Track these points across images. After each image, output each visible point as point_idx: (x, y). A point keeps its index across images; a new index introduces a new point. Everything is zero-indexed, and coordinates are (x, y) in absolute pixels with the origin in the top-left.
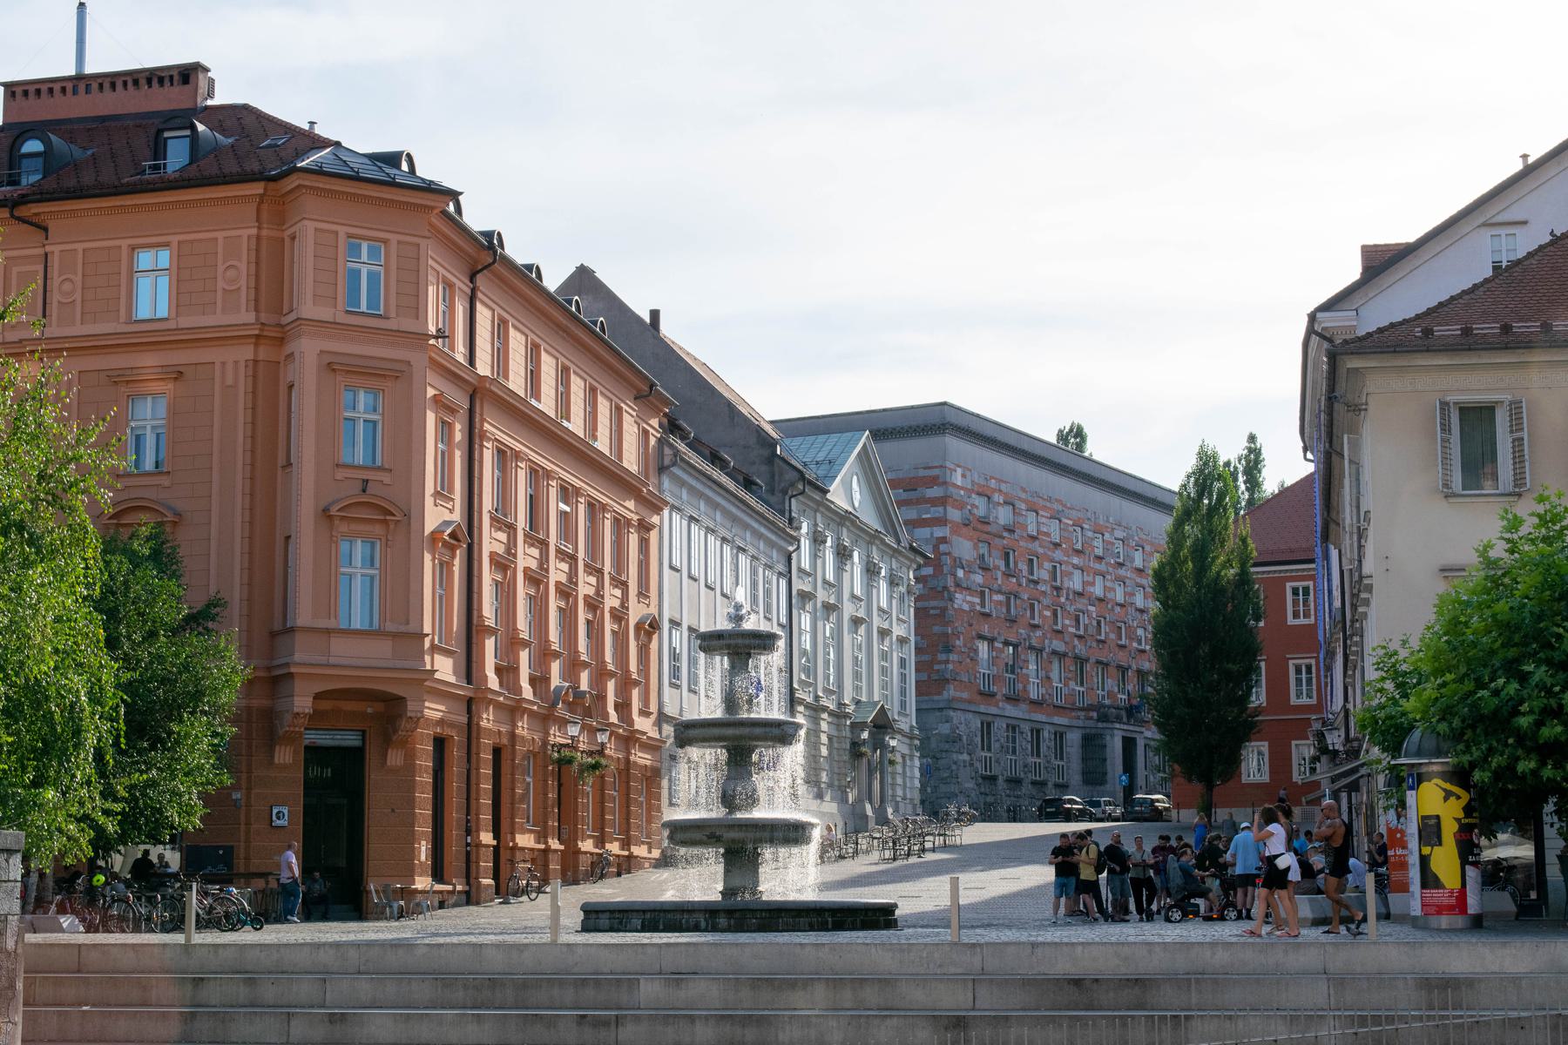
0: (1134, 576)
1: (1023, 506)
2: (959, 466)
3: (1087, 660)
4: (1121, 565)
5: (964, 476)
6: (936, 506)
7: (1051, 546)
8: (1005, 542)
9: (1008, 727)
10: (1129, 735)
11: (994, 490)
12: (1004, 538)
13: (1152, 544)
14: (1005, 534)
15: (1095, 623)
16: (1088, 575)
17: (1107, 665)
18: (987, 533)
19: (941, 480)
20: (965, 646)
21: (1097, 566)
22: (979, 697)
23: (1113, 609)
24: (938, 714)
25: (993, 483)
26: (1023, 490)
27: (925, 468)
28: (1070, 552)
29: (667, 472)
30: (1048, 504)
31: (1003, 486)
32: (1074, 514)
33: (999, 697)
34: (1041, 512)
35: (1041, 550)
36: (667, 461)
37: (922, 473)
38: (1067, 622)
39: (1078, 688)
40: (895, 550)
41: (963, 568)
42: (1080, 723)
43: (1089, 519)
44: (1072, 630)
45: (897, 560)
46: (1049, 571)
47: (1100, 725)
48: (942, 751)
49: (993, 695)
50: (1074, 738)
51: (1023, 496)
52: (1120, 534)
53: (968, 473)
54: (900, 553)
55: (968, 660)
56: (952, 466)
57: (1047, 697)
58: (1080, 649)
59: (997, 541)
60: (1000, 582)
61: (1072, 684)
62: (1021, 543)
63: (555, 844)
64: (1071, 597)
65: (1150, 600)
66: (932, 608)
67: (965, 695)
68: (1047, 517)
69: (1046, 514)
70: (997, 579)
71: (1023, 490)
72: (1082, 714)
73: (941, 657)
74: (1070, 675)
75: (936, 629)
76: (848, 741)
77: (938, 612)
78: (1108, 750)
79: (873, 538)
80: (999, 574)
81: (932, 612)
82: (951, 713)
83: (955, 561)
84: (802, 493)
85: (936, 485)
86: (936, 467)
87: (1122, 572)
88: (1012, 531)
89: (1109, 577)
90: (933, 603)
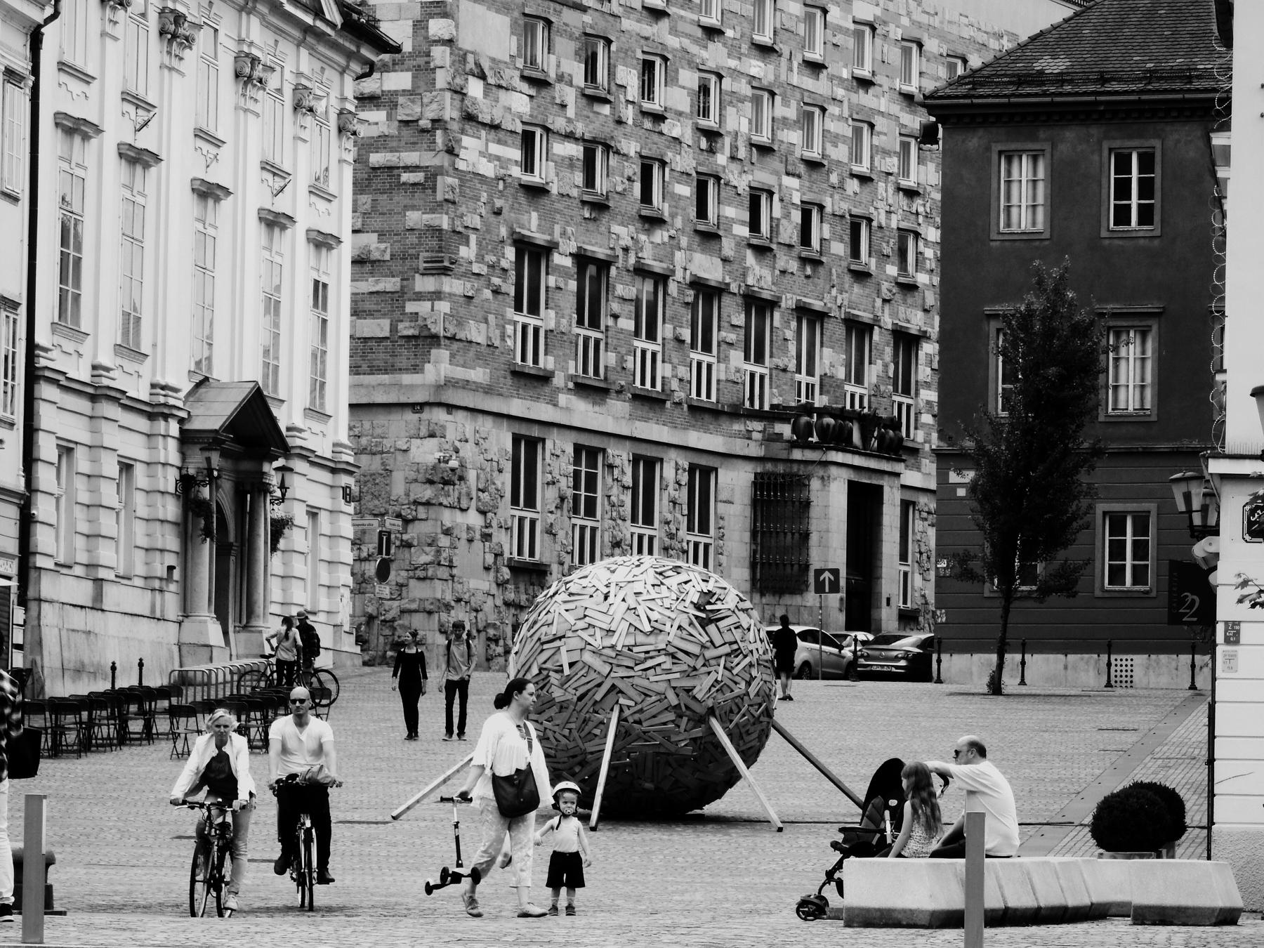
0: (896, 108)
3: (773, 304)
4: (865, 84)
7: (699, 33)
8: (587, 18)
9: (578, 449)
13: (942, 36)
15: (797, 216)
16: (786, 103)
20: (480, 258)
21: (808, 82)
22: (509, 381)
23: (842, 187)
24: (410, 416)
28: (745, 48)
33: (559, 380)
35: (673, 42)
38: (730, 212)
39: (751, 367)
40: (307, 30)
41: (482, 76)
42: (755, 450)
44: (744, 231)
46: (690, 91)
47: (797, 454)
48: (416, 503)
49: (544, 378)
54: (320, 36)
55: (487, 294)
57: (675, 385)
58: (760, 276)
60: (571, 112)
61: (736, 356)
62: (627, 24)
64: (742, 153)
65: (931, 167)
66: (407, 168)
67: (478, 375)
70: (563, 106)
72: (757, 426)
73: (424, 284)
74: (732, 337)
75: (414, 218)
77: (418, 177)
78: (815, 512)
80: (570, 96)
81: (405, 177)
82: (440, 415)
83: (464, 59)
87: (866, 99)
89: (833, 109)
90: (411, 158)
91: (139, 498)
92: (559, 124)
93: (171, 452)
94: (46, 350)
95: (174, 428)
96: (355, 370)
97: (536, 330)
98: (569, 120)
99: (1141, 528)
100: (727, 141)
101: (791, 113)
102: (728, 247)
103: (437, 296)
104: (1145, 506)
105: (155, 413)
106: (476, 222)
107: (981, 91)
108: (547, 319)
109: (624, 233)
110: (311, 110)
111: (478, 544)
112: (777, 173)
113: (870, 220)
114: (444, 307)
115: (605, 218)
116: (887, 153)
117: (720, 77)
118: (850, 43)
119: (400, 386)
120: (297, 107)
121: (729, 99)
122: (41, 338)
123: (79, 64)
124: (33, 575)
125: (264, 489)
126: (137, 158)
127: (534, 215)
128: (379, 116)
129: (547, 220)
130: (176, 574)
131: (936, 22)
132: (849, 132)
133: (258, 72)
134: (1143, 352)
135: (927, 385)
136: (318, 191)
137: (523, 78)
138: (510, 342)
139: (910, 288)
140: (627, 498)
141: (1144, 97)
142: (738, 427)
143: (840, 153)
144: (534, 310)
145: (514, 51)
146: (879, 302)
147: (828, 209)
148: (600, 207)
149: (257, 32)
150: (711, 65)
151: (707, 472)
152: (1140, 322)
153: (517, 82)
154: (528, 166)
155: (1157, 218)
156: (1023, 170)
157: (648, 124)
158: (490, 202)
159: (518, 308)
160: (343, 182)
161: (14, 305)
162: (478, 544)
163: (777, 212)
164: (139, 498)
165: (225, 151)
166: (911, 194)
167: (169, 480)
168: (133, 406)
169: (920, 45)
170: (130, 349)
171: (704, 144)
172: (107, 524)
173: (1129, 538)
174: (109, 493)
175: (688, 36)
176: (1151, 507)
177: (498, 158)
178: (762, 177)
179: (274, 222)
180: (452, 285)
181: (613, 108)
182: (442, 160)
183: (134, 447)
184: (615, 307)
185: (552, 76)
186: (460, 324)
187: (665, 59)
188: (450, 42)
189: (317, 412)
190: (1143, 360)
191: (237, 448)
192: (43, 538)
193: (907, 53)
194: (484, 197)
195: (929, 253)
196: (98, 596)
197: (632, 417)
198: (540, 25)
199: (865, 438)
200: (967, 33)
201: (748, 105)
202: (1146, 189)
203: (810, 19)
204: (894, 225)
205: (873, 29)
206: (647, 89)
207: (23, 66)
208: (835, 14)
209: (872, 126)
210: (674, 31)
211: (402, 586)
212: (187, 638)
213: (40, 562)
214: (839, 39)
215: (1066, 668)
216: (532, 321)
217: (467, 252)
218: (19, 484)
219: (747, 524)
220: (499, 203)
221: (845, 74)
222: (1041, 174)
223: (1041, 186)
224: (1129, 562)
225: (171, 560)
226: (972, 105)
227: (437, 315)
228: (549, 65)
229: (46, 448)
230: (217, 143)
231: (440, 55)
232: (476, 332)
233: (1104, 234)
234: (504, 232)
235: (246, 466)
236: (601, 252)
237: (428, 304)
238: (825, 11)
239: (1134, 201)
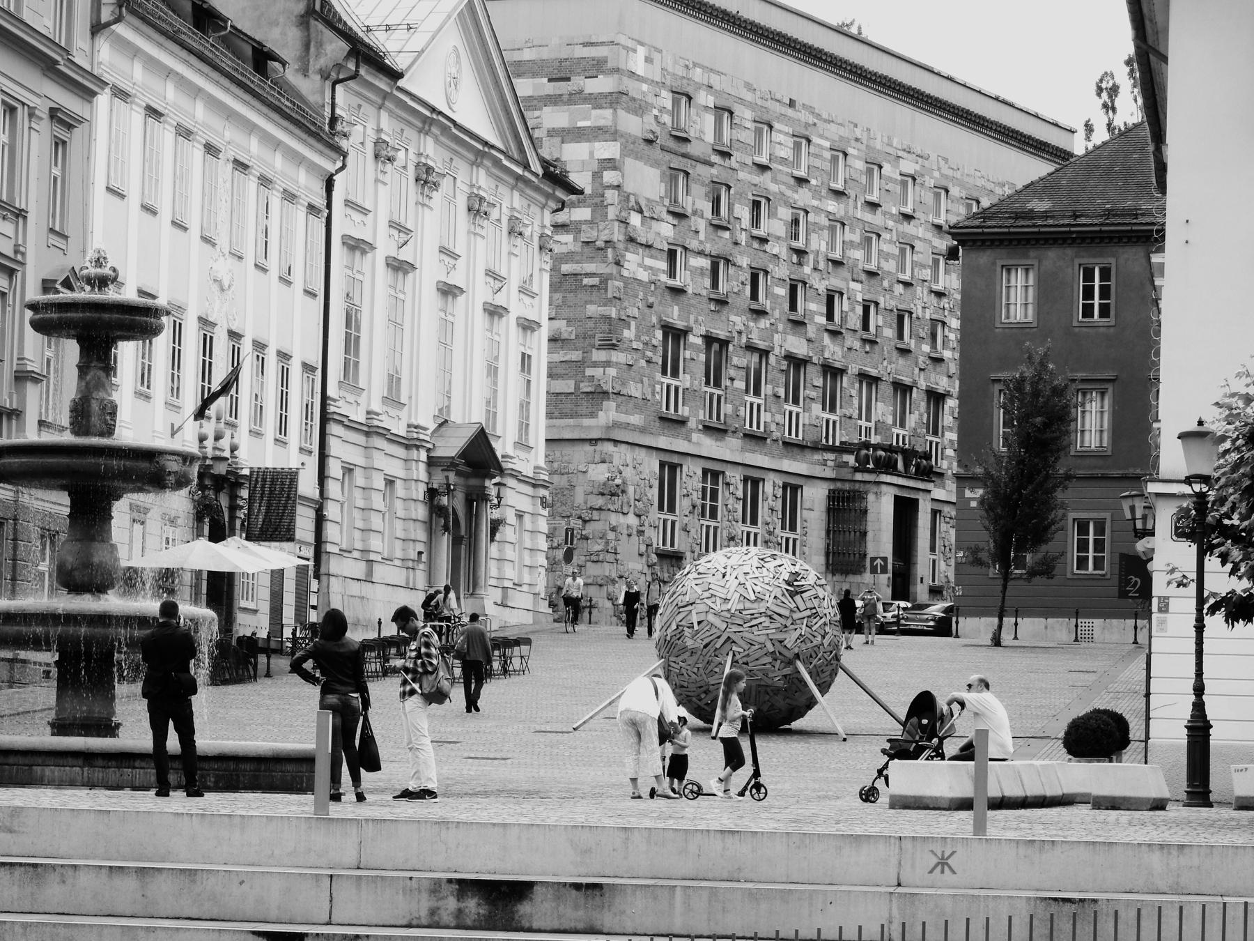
0: (930, 235)
1: (748, 114)
2: (642, 44)
3: (842, 371)
4: (908, 217)
5: (648, 60)
6: (601, 108)
7: (792, 181)
8: (714, 171)
9: (705, 472)
10: (906, 494)
11: (699, 86)
12: (712, 165)
13: (962, 185)
14: (715, 159)
16: (852, 231)
17: (876, 380)
18: (684, 156)
19: (610, 65)
20: (638, 338)
21: (868, 216)
22: (657, 424)
24: (588, 448)
25: (698, 75)
26: (749, 87)
27: (585, 44)
28: (824, 192)
29: (106, 32)
30: (790, 112)
31: (715, 80)
32: (833, 131)
33: (692, 424)
34: (776, 125)
35: (774, 188)
36: (106, 15)
37: (581, 52)
38: (813, 306)
40: (519, 178)
41: (641, 211)
42: (830, 474)
43: (857, 140)
44: (822, 320)
45: (522, 193)
46: (785, 222)
47: (859, 476)
48: (592, 508)
49: (682, 422)
50: (815, 498)
51: (748, 96)
52: (908, 166)
53: (657, 56)
54: (527, 182)
55: (643, 363)
56: (630, 44)
57: (773, 427)
58: (833, 352)
59: (701, 169)
60: (702, 236)
61: (816, 408)
64: (822, 266)
65: (954, 276)
66: (587, 275)
67: (636, 419)
68: (787, 134)
69: (786, 129)
70: (697, 232)
71: (749, 87)
72: (830, 456)
74: (813, 394)
75: (592, 310)
77: (595, 281)
79: (480, 152)
80: (701, 225)
81: (586, 281)
82: (609, 448)
84: (355, 76)
85: (603, 72)
86: (603, 43)
87: (909, 228)
88: (726, 155)
89: (885, 236)
90: (590, 267)
91: (399, 505)
92: (693, 244)
93: (421, 472)
94: (335, 400)
95: (423, 455)
96: (550, 415)
97: (677, 389)
98: (701, 242)
99: (1100, 530)
100: (811, 257)
101: (856, 237)
102: (811, 331)
103: (607, 364)
104: (1102, 515)
105: (410, 444)
106: (635, 312)
107: (989, 223)
108: (685, 381)
109: (738, 321)
110: (520, 234)
111: (635, 538)
112: (846, 280)
113: (911, 313)
114: (612, 372)
115: (726, 310)
116: (923, 266)
117: (807, 212)
118: (898, 189)
120: (511, 232)
121: (812, 228)
122: (331, 392)
123: (359, 201)
124: (324, 557)
125: (485, 498)
126: (399, 267)
127: (676, 308)
128: (567, 238)
129: (685, 312)
130: (424, 557)
131: (958, 175)
132: (897, 252)
133: (484, 207)
134: (1102, 407)
135: (950, 429)
136: (524, 290)
137: (669, 212)
138: (658, 397)
139: (938, 361)
140: (739, 507)
141: (1104, 228)
142: (817, 457)
143: (890, 266)
144: (675, 374)
145: (663, 194)
146: (917, 370)
147: (882, 305)
148: (722, 303)
149: (483, 180)
150: (800, 204)
151: (795, 489)
152: (1099, 385)
153: (665, 215)
154: (672, 273)
155: (1112, 313)
156: (1018, 279)
157: (756, 245)
158: (645, 299)
159: (664, 372)
160: (543, 284)
162: (635, 538)
163: (846, 308)
164: (399, 505)
165: (461, 263)
166: (940, 295)
167: (420, 492)
168: (394, 440)
169: (947, 191)
170: (393, 400)
171: (795, 258)
172: (376, 522)
173: (1091, 537)
174: (378, 501)
175: (784, 183)
176: (1107, 515)
177: (651, 268)
178: (835, 282)
179: (495, 312)
180: (618, 357)
181: (732, 234)
182: (613, 269)
183: (395, 468)
184: (732, 372)
185: (689, 211)
186: (623, 384)
187: (769, 200)
188: (618, 187)
189: (522, 445)
190: (1102, 412)
191: (468, 469)
192: (331, 532)
193: (937, 196)
194: (641, 295)
195: (952, 336)
196: (370, 572)
197: (743, 450)
198: (681, 175)
199: (906, 466)
200: (980, 183)
201: (826, 232)
202: (1105, 292)
203: (870, 172)
204: (928, 317)
205: (914, 179)
206: (756, 221)
207: (320, 202)
208: (887, 169)
209: (913, 247)
210: (774, 180)
213: (329, 548)
214: (890, 186)
215: (1046, 627)
216: (674, 382)
217: (628, 334)
219: (823, 525)
220: (651, 300)
221: (894, 211)
222: (1031, 282)
223: (1031, 290)
224: (1091, 554)
225: (421, 547)
226: (983, 233)
227: (607, 377)
228: (687, 203)
229: (334, 468)
230: (455, 257)
231: (611, 196)
232: (634, 390)
233: (1075, 324)
234: (654, 320)
235: (474, 482)
236: (722, 334)
237: (601, 370)
238: (880, 167)
239: (1097, 301)
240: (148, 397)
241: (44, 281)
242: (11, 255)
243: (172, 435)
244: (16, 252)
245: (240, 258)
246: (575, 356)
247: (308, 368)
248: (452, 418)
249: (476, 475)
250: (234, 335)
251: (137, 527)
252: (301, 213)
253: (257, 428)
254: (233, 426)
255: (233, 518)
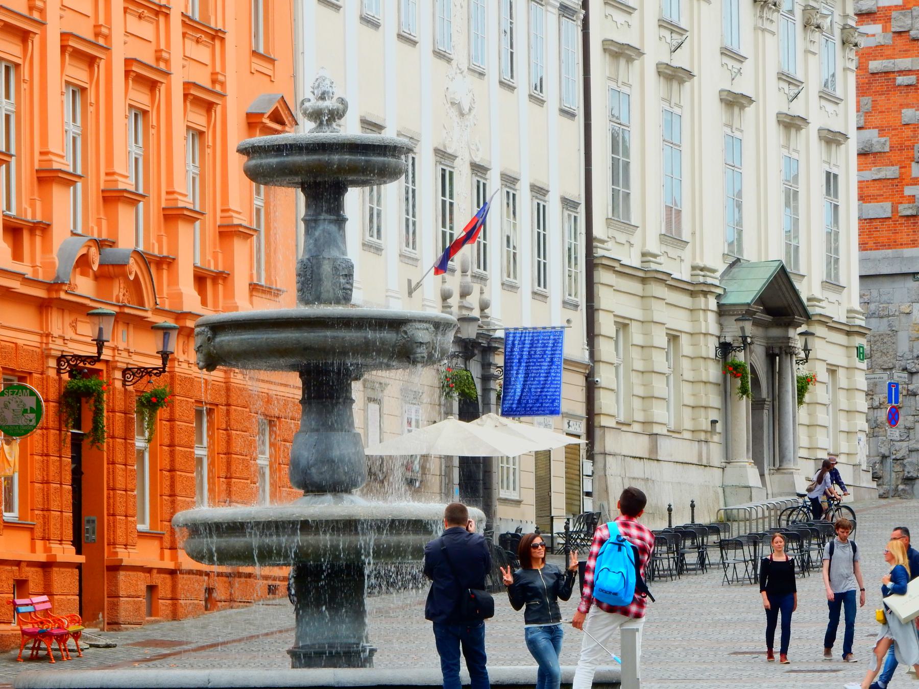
63: (66, 553)
66: (901, 72)
76: (713, 343)
81: (900, 80)
91: (685, 364)
93: (710, 323)
94: (603, 242)
95: (712, 303)
96: (863, 246)
105: (696, 290)
110: (818, 27)
119: (902, 259)
120: (806, 25)
122: (599, 230)
124: (598, 433)
125: (789, 351)
128: (875, 29)
130: (719, 427)
136: (827, 96)
160: (847, 87)
161: (573, 205)
164: (685, 364)
165: (748, 66)
167: (710, 347)
168: (677, 286)
172: (659, 386)
183: (680, 321)
189: (832, 284)
191: (768, 318)
192: (605, 401)
196: (654, 448)
211: (909, 429)
212: (729, 482)
213: (604, 421)
218: (585, 357)
225: (714, 415)
229: (606, 324)
230: (740, 59)
235: (776, 332)
240: (378, 250)
241: (249, 115)
242: (208, 86)
243: (410, 293)
244: (214, 82)
245: (482, 74)
246: (891, 172)
247: (568, 203)
248: (746, 256)
249: (778, 325)
250: (478, 169)
251: (374, 407)
252: (552, 16)
253: (511, 279)
254: (482, 279)
255: (486, 390)
